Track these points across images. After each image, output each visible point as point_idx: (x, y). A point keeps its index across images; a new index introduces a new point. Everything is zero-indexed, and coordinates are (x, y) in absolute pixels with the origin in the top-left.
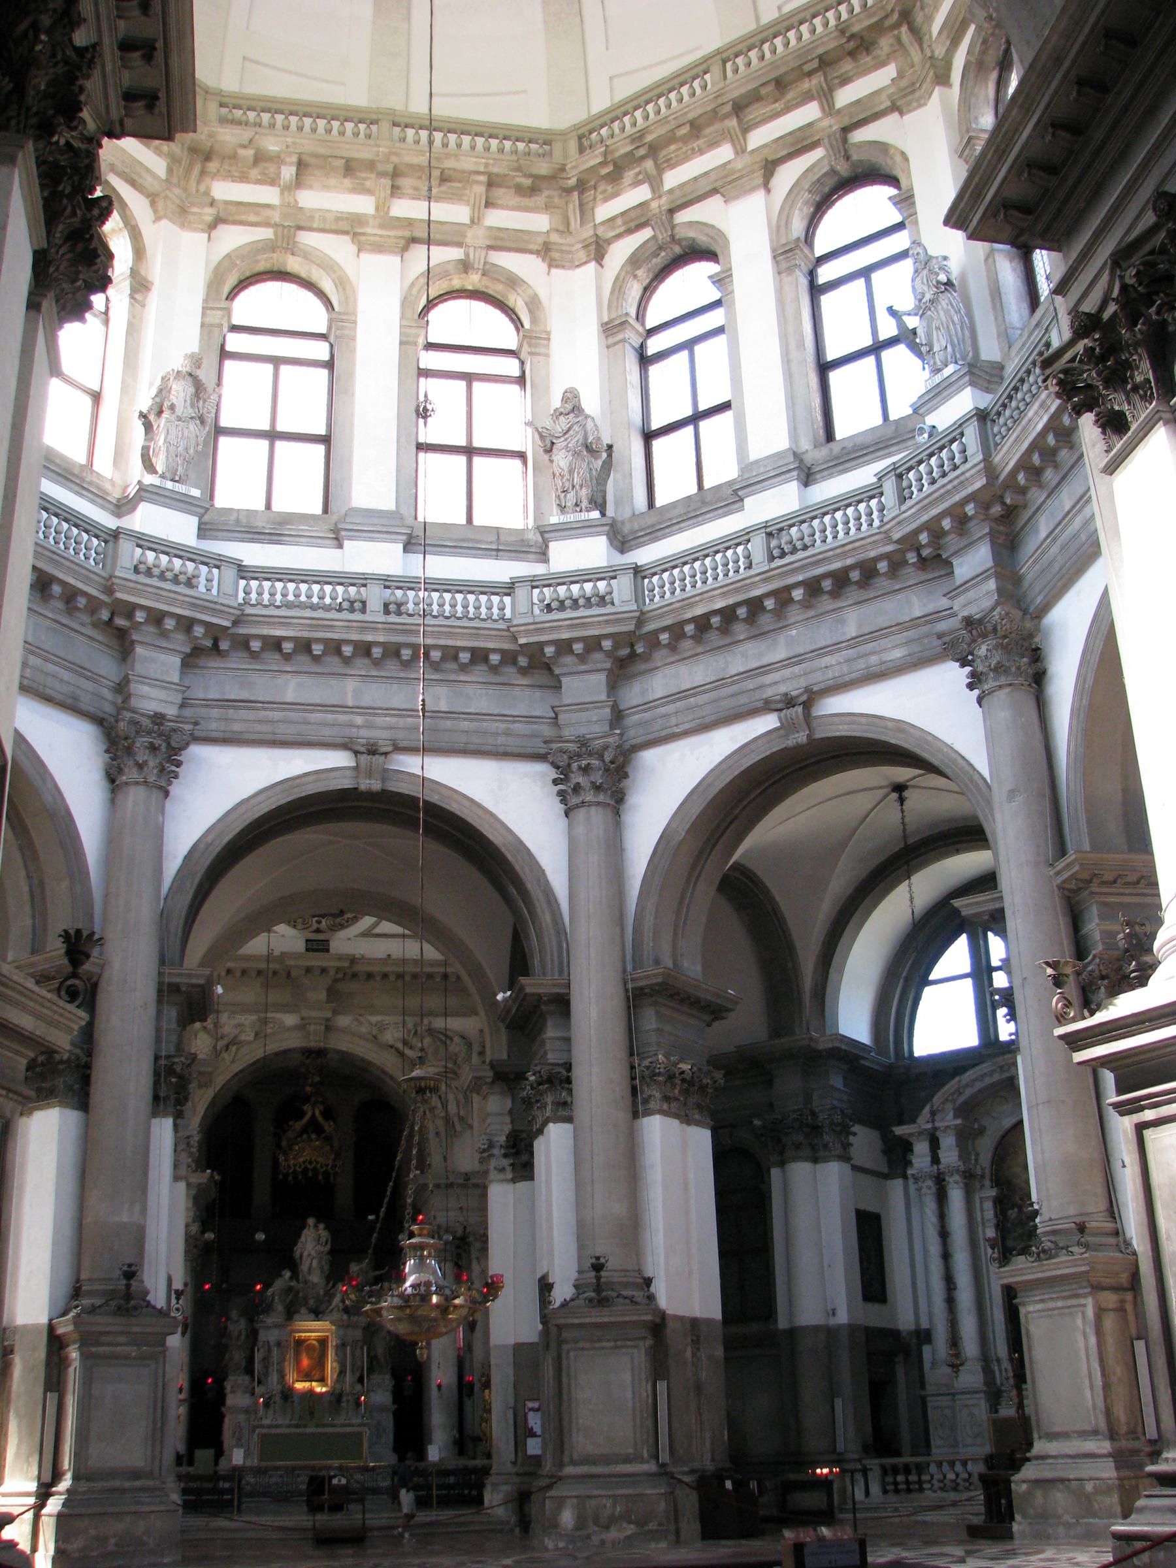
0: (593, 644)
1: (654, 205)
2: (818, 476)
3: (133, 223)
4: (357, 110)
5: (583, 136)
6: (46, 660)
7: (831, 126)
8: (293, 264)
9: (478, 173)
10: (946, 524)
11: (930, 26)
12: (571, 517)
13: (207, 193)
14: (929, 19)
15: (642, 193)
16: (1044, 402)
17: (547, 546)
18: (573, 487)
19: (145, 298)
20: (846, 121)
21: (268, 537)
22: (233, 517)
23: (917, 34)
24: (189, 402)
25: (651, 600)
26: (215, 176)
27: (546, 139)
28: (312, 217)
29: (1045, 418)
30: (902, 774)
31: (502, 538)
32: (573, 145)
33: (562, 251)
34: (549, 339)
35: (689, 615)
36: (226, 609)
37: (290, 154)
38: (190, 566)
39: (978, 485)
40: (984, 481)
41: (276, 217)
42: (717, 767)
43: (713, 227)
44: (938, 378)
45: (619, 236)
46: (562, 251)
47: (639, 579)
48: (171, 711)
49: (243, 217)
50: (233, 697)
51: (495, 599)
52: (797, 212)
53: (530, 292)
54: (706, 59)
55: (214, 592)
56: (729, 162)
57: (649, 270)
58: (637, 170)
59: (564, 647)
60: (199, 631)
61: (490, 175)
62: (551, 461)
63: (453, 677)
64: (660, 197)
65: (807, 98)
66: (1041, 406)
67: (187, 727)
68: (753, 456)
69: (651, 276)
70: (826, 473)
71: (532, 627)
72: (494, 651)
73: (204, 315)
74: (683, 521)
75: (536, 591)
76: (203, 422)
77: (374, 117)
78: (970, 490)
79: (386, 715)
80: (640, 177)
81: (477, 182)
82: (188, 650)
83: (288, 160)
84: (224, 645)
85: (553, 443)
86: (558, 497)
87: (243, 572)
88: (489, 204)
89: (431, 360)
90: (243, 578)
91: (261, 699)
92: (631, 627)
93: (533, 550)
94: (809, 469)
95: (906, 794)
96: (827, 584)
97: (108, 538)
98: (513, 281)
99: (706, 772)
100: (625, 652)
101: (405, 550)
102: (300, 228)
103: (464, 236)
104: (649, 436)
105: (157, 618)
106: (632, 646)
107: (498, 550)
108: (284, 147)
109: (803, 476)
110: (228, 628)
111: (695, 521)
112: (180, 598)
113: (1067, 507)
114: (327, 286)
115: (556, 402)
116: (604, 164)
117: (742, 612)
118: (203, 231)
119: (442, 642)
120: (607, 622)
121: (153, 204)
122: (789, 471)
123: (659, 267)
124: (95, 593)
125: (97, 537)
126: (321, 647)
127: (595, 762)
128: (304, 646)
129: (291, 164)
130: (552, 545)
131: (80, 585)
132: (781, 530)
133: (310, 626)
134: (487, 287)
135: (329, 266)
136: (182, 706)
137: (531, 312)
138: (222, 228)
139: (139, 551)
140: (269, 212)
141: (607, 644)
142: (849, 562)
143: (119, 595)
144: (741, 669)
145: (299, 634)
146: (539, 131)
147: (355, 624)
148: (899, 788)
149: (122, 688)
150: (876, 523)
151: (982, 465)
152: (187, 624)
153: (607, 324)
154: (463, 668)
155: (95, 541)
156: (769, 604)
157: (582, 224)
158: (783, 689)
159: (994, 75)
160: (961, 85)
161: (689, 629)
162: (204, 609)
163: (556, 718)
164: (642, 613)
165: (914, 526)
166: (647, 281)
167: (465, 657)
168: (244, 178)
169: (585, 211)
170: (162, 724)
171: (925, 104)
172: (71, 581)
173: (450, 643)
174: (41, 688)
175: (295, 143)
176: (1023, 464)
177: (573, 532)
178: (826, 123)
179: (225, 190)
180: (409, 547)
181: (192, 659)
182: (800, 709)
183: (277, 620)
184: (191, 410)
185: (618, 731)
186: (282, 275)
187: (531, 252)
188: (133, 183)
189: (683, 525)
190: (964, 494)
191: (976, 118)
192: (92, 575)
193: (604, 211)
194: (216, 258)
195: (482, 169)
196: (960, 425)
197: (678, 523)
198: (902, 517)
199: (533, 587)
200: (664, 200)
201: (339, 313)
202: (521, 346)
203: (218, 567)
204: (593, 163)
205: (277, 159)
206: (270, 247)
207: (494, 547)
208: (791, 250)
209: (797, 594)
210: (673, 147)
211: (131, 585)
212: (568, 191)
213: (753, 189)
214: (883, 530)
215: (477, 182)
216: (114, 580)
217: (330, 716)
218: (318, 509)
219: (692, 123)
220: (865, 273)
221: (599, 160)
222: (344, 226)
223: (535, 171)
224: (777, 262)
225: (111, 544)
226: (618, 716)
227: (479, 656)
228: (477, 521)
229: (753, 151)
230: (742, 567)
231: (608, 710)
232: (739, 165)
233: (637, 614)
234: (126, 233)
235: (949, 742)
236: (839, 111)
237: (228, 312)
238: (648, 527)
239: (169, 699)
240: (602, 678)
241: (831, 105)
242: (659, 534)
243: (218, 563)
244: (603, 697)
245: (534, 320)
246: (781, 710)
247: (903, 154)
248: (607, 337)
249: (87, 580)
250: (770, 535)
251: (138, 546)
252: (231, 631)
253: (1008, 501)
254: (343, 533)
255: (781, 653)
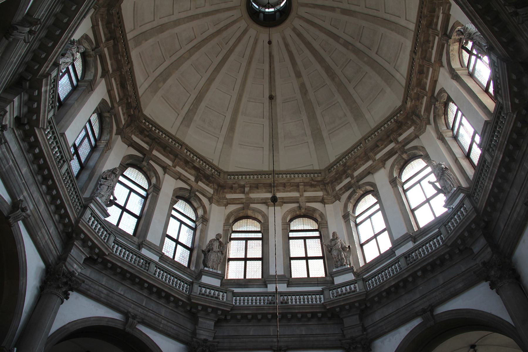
0: (352, 305)
1: (352, 181)
2: (418, 239)
3: (203, 205)
4: (265, 171)
5: (329, 169)
6: (168, 322)
7: (399, 146)
8: (250, 213)
9: (301, 182)
10: (466, 234)
11: (421, 113)
12: (340, 269)
13: (225, 197)
14: (420, 111)
15: (349, 180)
16: (489, 177)
17: (334, 280)
18: (339, 260)
19: (207, 223)
20: (403, 144)
21: (243, 286)
22: (233, 282)
23: (419, 116)
24: (217, 247)
25: (370, 288)
26: (226, 193)
27: (319, 172)
28: (255, 200)
29: (492, 183)
30: (472, 336)
31: (319, 280)
32: (327, 172)
33: (327, 200)
34: (327, 223)
35: (383, 289)
36: (228, 305)
37: (247, 184)
38: (217, 293)
39: (474, 217)
40: (476, 214)
41: (244, 201)
42: (403, 340)
43: (371, 182)
44: (450, 194)
45: (344, 193)
46: (327, 200)
47: (365, 282)
48: (211, 339)
49: (235, 202)
50: (232, 335)
51: (318, 296)
52: (394, 171)
53: (319, 212)
54: (360, 140)
55: (225, 300)
56: (372, 164)
57: (354, 200)
58: (346, 174)
59: (342, 308)
60: (220, 312)
61: (304, 182)
62: (332, 254)
63: (306, 323)
64: (354, 179)
65: (391, 142)
66: (489, 179)
67: (215, 344)
68: (395, 239)
69: (355, 202)
70: (420, 237)
71: (330, 302)
72: (319, 312)
73: (224, 227)
74: (377, 264)
75: (331, 292)
76: (222, 254)
77: (270, 173)
78: (471, 219)
79: (284, 337)
80: (347, 176)
81: (301, 185)
82: (216, 320)
83: (247, 186)
84: (229, 317)
85: (331, 249)
86: (335, 264)
87: (235, 294)
88: (305, 191)
89: (291, 235)
90: (234, 296)
91: (241, 335)
92: (364, 297)
93: (329, 282)
94: (414, 237)
95: (476, 348)
96: (429, 268)
97: (190, 284)
98: (315, 210)
99: (399, 343)
100: (363, 307)
101: (288, 286)
102: (252, 203)
103: (299, 199)
104: (362, 246)
105: (205, 308)
106: (366, 304)
107: (318, 284)
108: (245, 183)
109: (413, 239)
110: (229, 311)
111: (380, 263)
112: (213, 301)
113: (509, 213)
114: (260, 218)
115: (331, 237)
116: (336, 174)
117: (401, 284)
118: (224, 206)
119: (301, 311)
120: (356, 297)
121: (209, 200)
122: (408, 238)
123: (357, 199)
124: (185, 300)
125: (186, 284)
126: (261, 316)
127: (359, 346)
128: (254, 316)
129: (248, 187)
130: (335, 279)
131: (180, 297)
132: (409, 255)
133: (257, 309)
134: (307, 213)
135: (260, 212)
136: (214, 338)
137: (321, 217)
138: (229, 205)
139: (199, 288)
140: (242, 200)
141: (357, 304)
142: (435, 258)
143: (192, 301)
144: (405, 304)
145: (253, 312)
146: (317, 170)
147: (271, 307)
148: (473, 346)
149: (194, 333)
150: (441, 243)
151: (473, 209)
152: (215, 310)
153: (344, 215)
154: (309, 320)
155: (186, 285)
156: (410, 279)
157: (333, 192)
158: (421, 308)
159: (443, 117)
160: (434, 122)
161: (384, 294)
162: (221, 305)
163: (343, 333)
164: (367, 292)
165: (455, 238)
166: (354, 203)
167: (309, 315)
168: (235, 193)
169: (334, 189)
170: (207, 343)
171: (425, 132)
172: (177, 296)
173: (304, 311)
174: (166, 331)
175: (248, 181)
176: (488, 203)
177: (342, 273)
178: (397, 146)
179: (229, 196)
180: (289, 285)
181: (218, 323)
182: (429, 313)
183: (245, 308)
184: (218, 250)
185: (365, 333)
186: (247, 217)
187: (319, 202)
188: (204, 195)
189: (377, 265)
190: (469, 222)
191: (441, 129)
192: (183, 294)
193: (338, 188)
194: (227, 213)
195: (302, 181)
196: (462, 201)
197: (375, 265)
198: (449, 237)
199: (330, 290)
200: (355, 179)
201: (263, 223)
202: (319, 227)
203: (226, 293)
204: (333, 175)
205: (244, 187)
206: (243, 209)
207: (317, 283)
208: (395, 180)
209: (419, 274)
210: (355, 166)
211: (197, 297)
212: (328, 184)
213: (380, 168)
214: (444, 243)
215: (301, 185)
216: (191, 296)
217: (265, 339)
218: (260, 277)
219: (359, 156)
220: (419, 182)
221: (334, 174)
222: (264, 201)
223: (317, 180)
224: (391, 185)
225: (191, 286)
226: (364, 329)
227: (314, 315)
228: (311, 276)
229: (378, 159)
230: (399, 270)
231: (361, 327)
232: (375, 164)
233: (366, 292)
234: (201, 207)
235: (489, 312)
236: (400, 142)
237: (232, 229)
238: (365, 269)
239: (210, 335)
240: (357, 317)
241: (398, 141)
242: (370, 270)
243: (226, 291)
244: (359, 323)
245: (322, 219)
246: (422, 315)
247: (422, 147)
248: (344, 220)
249: (182, 296)
250: (406, 258)
251: (200, 286)
252: (230, 313)
253: (486, 220)
254: (267, 282)
255: (418, 296)
